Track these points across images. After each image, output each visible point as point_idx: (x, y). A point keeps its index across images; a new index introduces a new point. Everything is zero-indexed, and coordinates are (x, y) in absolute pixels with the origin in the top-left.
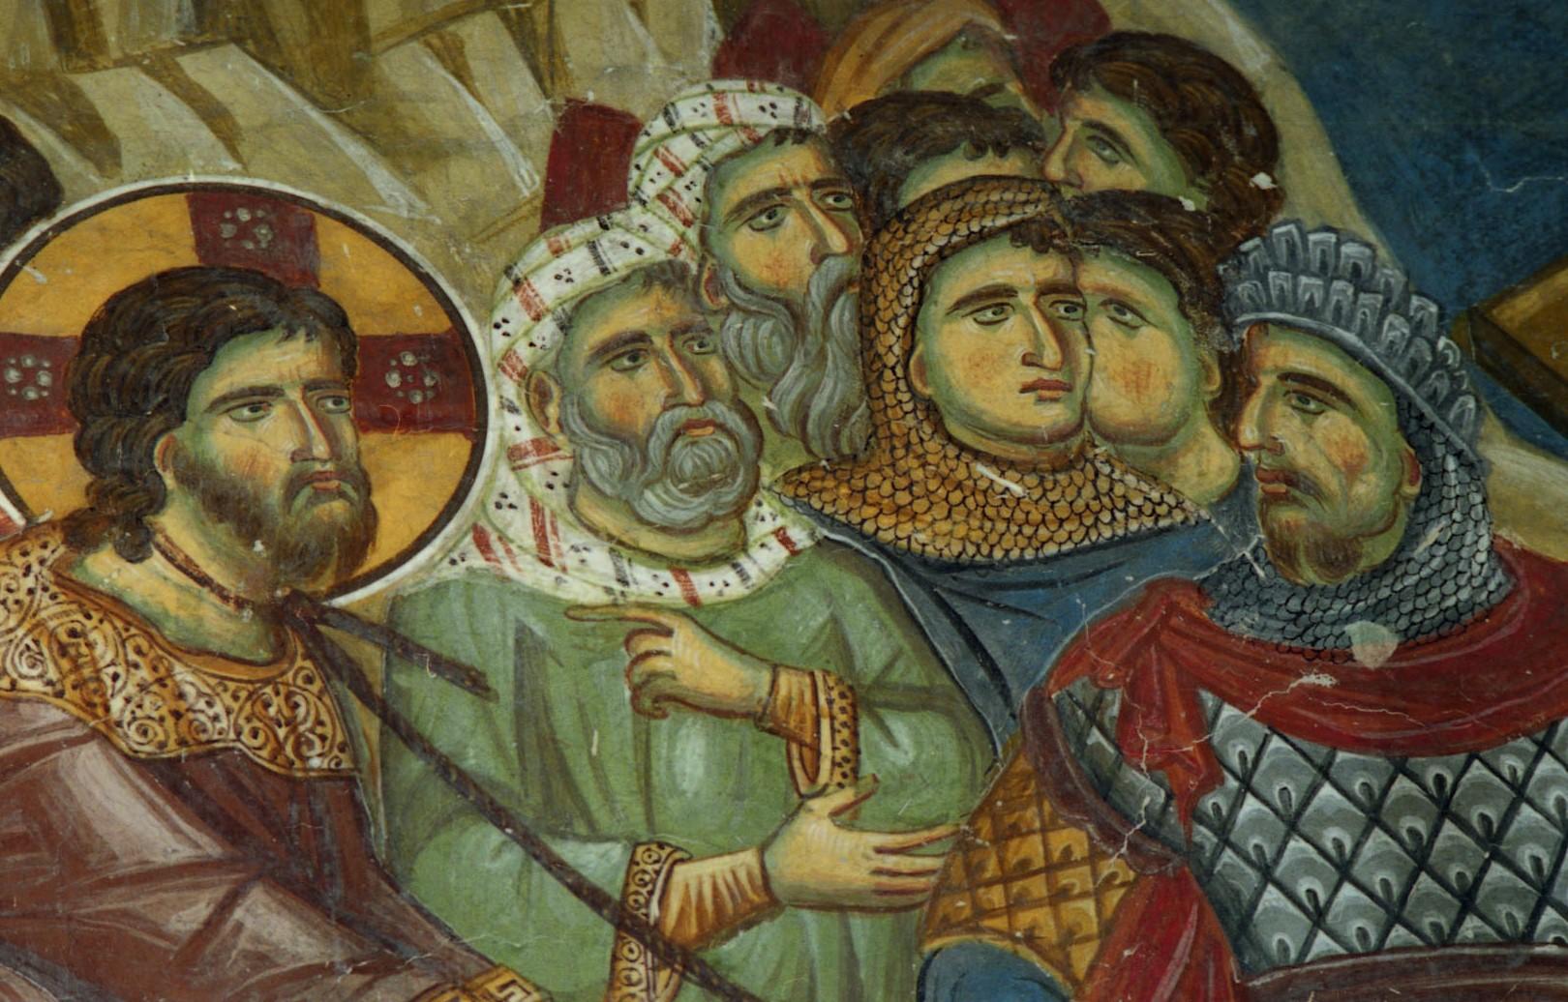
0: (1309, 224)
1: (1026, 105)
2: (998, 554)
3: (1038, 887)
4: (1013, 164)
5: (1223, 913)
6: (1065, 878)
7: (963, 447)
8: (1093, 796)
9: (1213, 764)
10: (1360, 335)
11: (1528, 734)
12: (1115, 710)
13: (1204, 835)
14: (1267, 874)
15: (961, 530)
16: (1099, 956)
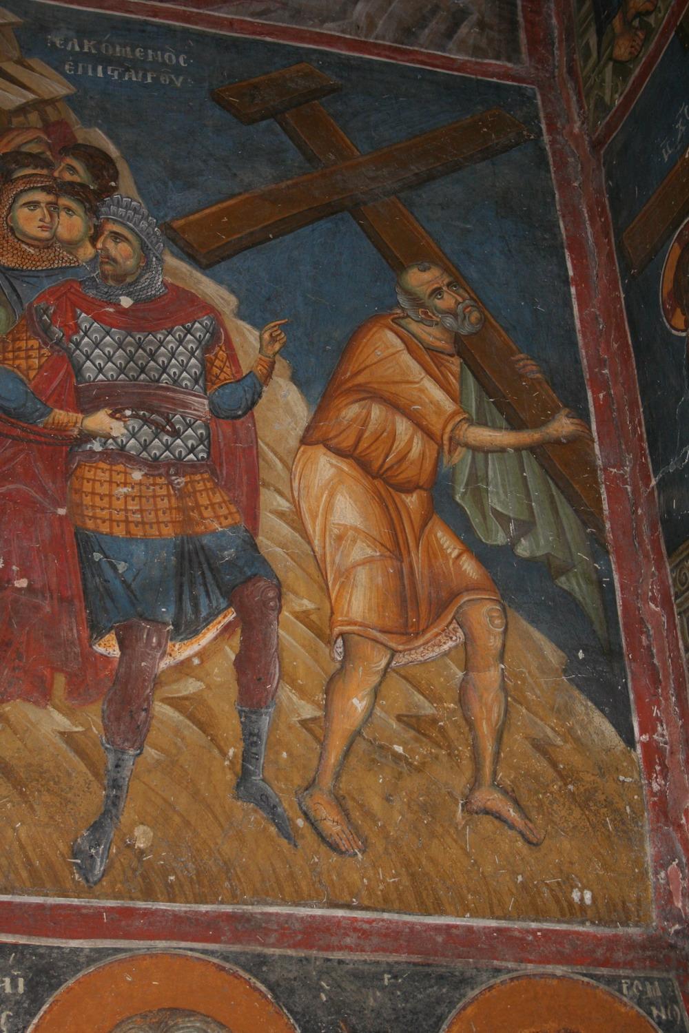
0: (124, 195)
1: (51, 157)
2: (25, 268)
3: (23, 354)
4: (45, 172)
5: (73, 367)
6: (30, 353)
7: (19, 240)
8: (45, 333)
9: (78, 327)
10: (134, 224)
11: (166, 329)
12: (52, 311)
13: (72, 346)
14: (88, 357)
15: (15, 261)
16: (37, 374)
